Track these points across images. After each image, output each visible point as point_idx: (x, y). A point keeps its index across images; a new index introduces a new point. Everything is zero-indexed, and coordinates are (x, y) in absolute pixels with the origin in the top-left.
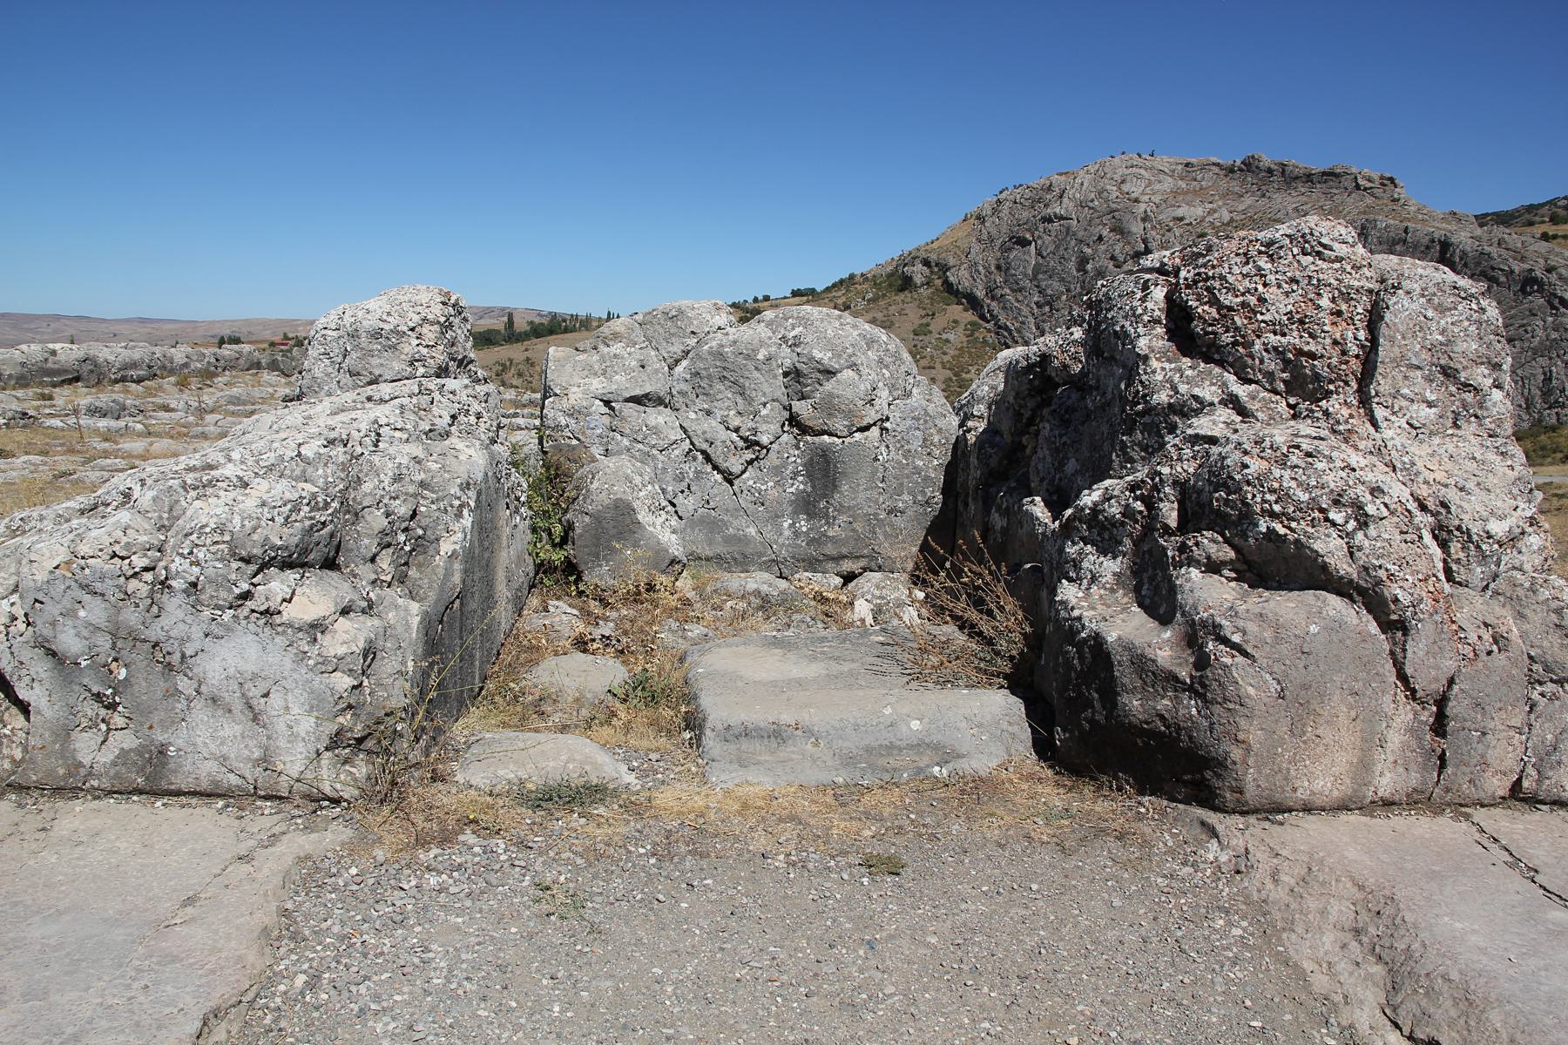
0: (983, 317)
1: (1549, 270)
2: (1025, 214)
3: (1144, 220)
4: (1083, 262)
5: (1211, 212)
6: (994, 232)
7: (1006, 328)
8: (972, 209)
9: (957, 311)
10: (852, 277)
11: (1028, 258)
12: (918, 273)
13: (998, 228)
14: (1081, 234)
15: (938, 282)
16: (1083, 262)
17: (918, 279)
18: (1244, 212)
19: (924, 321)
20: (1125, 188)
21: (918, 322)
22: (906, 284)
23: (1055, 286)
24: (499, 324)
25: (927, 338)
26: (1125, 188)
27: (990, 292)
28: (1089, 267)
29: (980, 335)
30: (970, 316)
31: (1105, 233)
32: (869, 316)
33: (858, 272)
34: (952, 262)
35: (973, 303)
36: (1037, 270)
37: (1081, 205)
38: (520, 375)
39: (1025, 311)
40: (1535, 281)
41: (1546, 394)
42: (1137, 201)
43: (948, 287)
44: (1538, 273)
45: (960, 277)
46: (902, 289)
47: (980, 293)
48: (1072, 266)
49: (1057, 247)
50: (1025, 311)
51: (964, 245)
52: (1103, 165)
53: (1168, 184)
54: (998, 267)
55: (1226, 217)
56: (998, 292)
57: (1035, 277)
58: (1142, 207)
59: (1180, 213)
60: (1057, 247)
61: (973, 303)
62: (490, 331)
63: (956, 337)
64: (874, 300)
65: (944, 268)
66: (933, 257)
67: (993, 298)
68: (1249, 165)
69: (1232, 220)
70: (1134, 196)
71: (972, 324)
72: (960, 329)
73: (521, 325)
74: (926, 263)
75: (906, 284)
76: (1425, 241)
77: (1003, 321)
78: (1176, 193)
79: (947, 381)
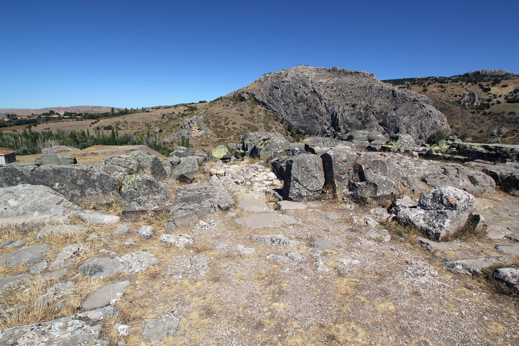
0: (267, 108)
1: (418, 98)
2: (275, 81)
3: (312, 83)
4: (296, 94)
5: (328, 81)
6: (267, 85)
7: (276, 112)
8: (258, 79)
9: (259, 107)
10: (221, 97)
11: (278, 93)
12: (246, 96)
13: (268, 84)
14: (294, 86)
15: (253, 99)
16: (296, 94)
17: (246, 98)
18: (336, 81)
19: (252, 109)
20: (304, 74)
21: (250, 110)
22: (242, 99)
23: (288, 100)
24: (110, 111)
25: (254, 114)
26: (304, 74)
27: (269, 101)
28: (298, 95)
29: (268, 113)
30: (263, 108)
31: (301, 86)
32: (236, 108)
33: (223, 96)
34: (255, 93)
35: (264, 104)
36: (282, 96)
37: (293, 78)
38: (124, 126)
39: (280, 107)
40: (416, 101)
41: (421, 128)
42: (308, 77)
43: (256, 100)
44: (417, 99)
45: (259, 97)
46: (242, 101)
47: (266, 102)
48: (293, 94)
49: (287, 90)
50: (280, 107)
51: (258, 88)
52: (297, 68)
53: (314, 74)
54: (270, 95)
55: (333, 83)
56: (271, 102)
57: (282, 97)
58: (310, 79)
59: (321, 81)
60: (287, 90)
61: (264, 104)
62: (106, 113)
63: (262, 114)
64: (234, 104)
65: (253, 95)
66: (250, 92)
67: (270, 103)
68: (334, 70)
69: (334, 84)
70: (307, 76)
71: (265, 110)
72: (262, 111)
73: (116, 111)
74: (247, 93)
75: (242, 99)
76: (388, 90)
77: (274, 110)
78: (317, 75)
79: (264, 126)
